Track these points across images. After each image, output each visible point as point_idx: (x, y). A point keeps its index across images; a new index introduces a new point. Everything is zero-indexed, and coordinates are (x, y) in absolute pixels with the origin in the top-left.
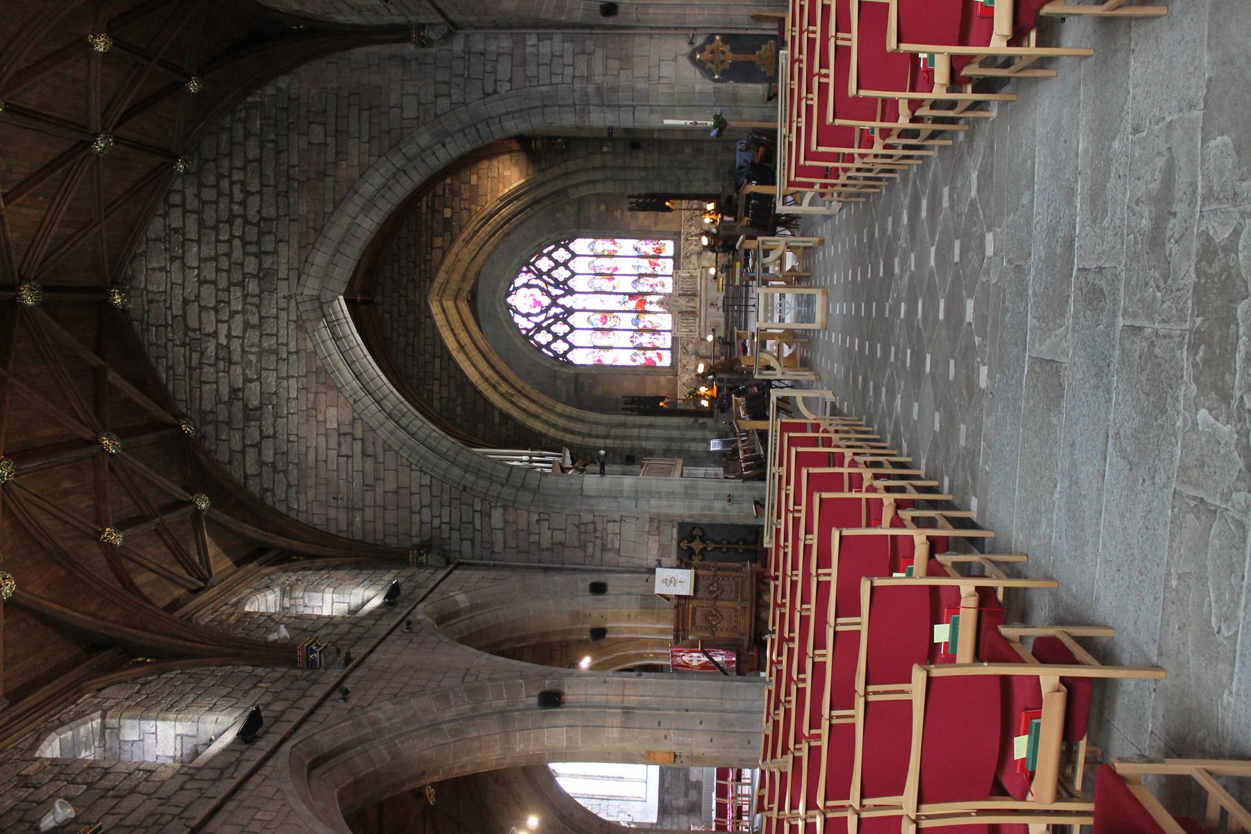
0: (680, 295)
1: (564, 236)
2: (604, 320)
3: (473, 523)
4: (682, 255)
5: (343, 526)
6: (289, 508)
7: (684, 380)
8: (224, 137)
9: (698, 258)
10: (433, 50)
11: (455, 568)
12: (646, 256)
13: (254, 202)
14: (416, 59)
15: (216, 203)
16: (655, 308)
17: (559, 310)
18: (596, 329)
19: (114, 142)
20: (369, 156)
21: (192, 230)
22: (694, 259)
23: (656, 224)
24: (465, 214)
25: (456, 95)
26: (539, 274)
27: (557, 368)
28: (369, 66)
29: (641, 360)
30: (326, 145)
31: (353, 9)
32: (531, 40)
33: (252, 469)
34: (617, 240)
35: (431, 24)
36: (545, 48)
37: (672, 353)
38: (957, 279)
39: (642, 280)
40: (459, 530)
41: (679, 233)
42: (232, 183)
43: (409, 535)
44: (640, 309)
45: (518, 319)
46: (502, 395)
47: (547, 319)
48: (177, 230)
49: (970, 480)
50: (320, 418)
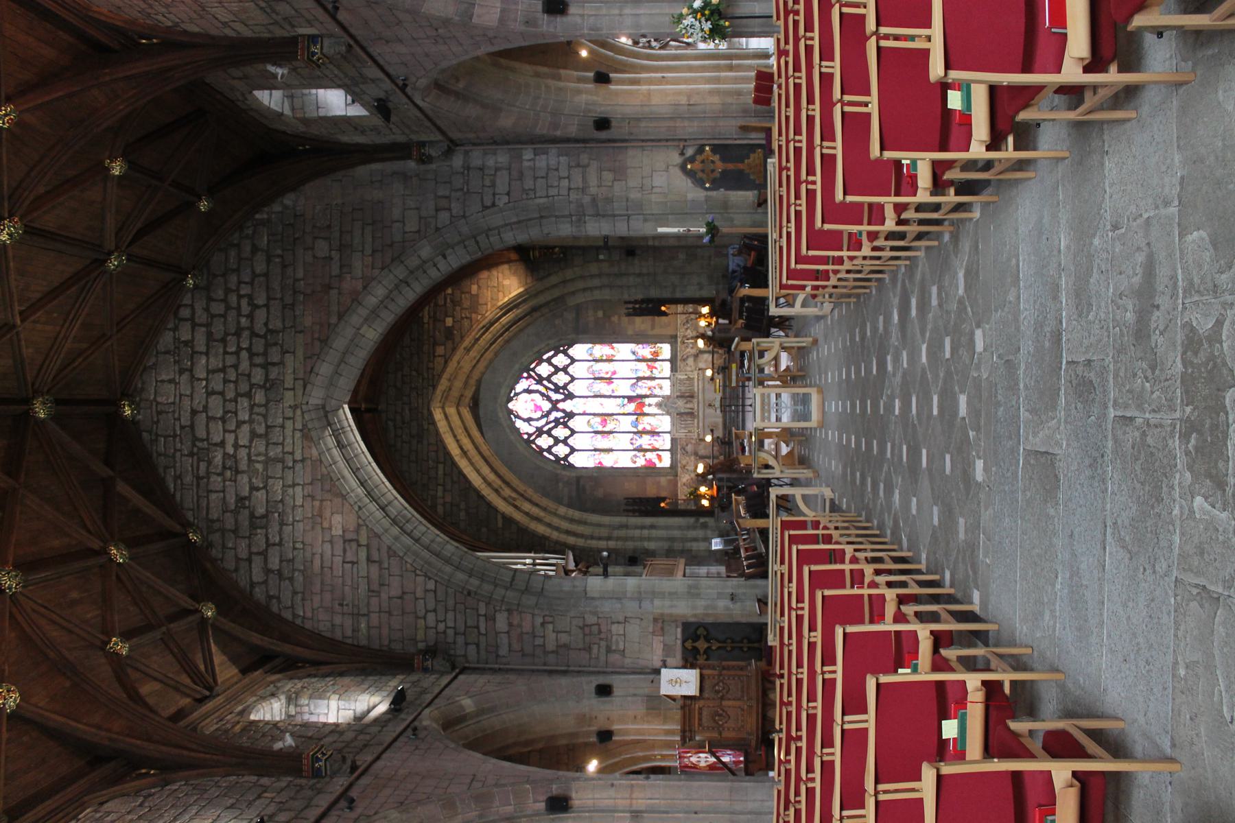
0: (677, 397)
1: (562, 342)
2: (604, 423)
3: (477, 627)
4: (679, 358)
5: (349, 633)
6: (295, 615)
7: (684, 480)
8: (233, 253)
9: (695, 360)
10: (433, 166)
11: (461, 673)
12: (643, 360)
13: (261, 315)
14: (417, 175)
15: (224, 316)
16: (654, 410)
17: (560, 415)
18: (596, 432)
19: (128, 259)
20: (373, 268)
21: (200, 343)
22: (690, 361)
23: (653, 328)
24: (466, 323)
25: (456, 208)
26: (540, 380)
27: (559, 472)
28: (372, 182)
29: (641, 462)
30: (331, 258)
31: (356, 129)
32: (528, 155)
33: (258, 576)
34: (614, 345)
35: (431, 143)
36: (542, 162)
37: (672, 455)
38: (949, 374)
39: (640, 383)
40: (464, 634)
41: (675, 337)
42: (240, 297)
43: (414, 641)
45: (519, 424)
46: (505, 499)
47: (547, 423)
48: (186, 343)
49: (971, 573)
50: (326, 525)
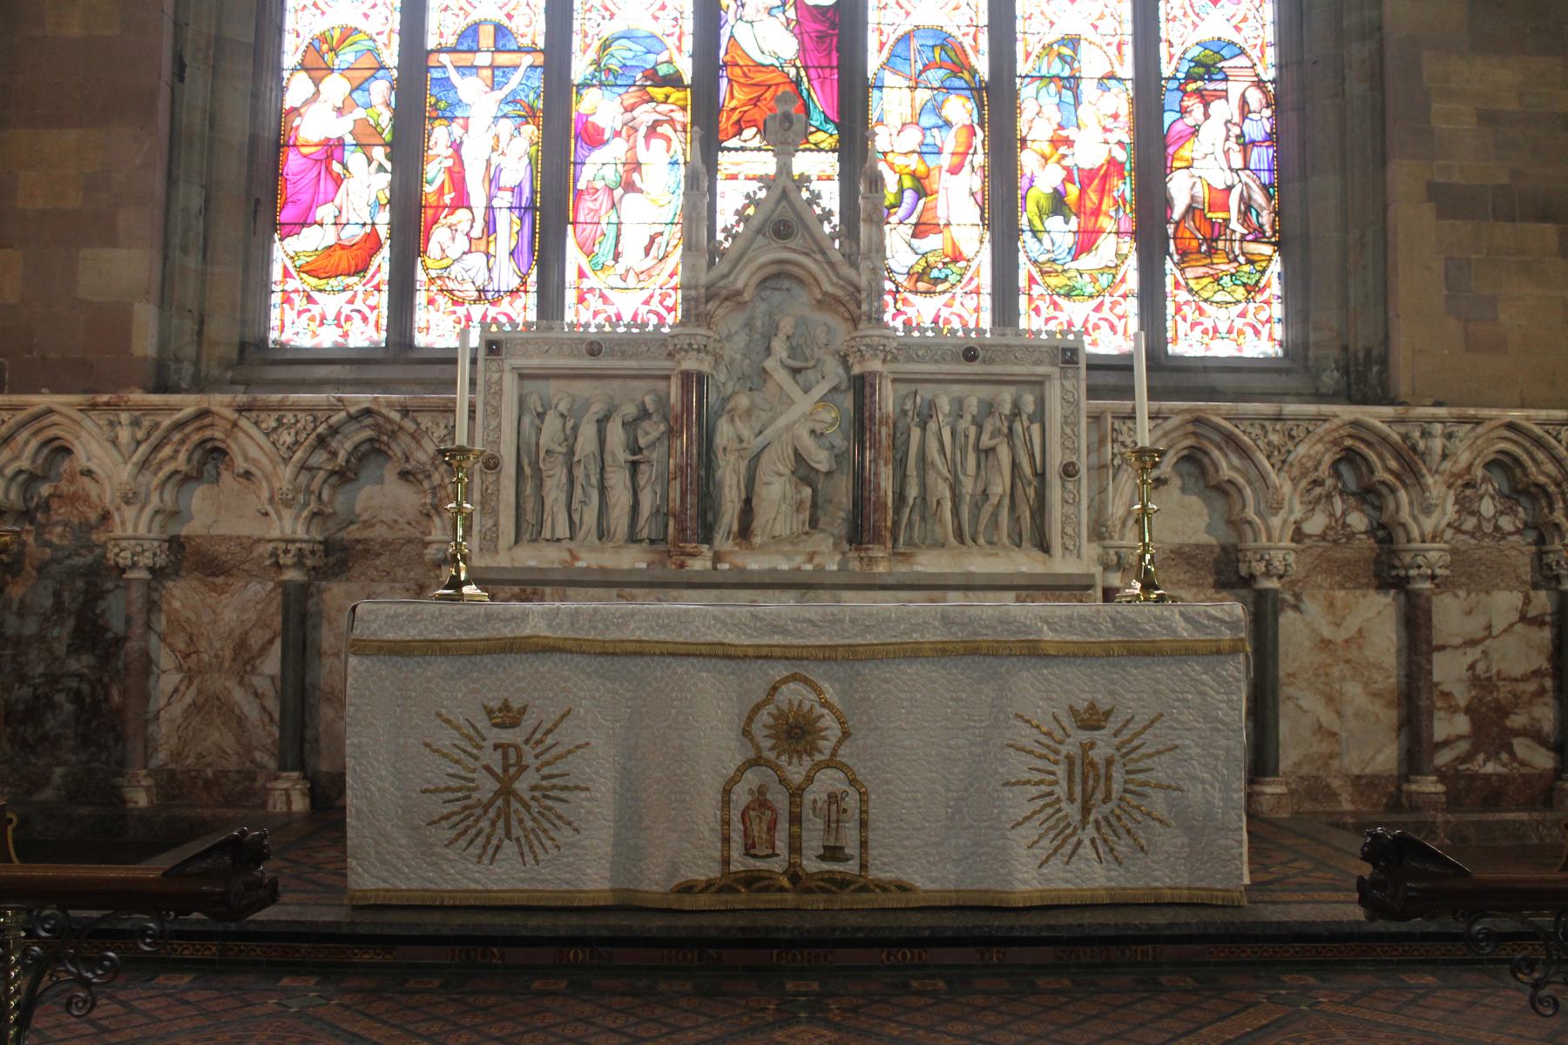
0: (861, 386)
4: (1218, 411)
9: (1184, 556)
39: (960, 109)
44: (731, 96)
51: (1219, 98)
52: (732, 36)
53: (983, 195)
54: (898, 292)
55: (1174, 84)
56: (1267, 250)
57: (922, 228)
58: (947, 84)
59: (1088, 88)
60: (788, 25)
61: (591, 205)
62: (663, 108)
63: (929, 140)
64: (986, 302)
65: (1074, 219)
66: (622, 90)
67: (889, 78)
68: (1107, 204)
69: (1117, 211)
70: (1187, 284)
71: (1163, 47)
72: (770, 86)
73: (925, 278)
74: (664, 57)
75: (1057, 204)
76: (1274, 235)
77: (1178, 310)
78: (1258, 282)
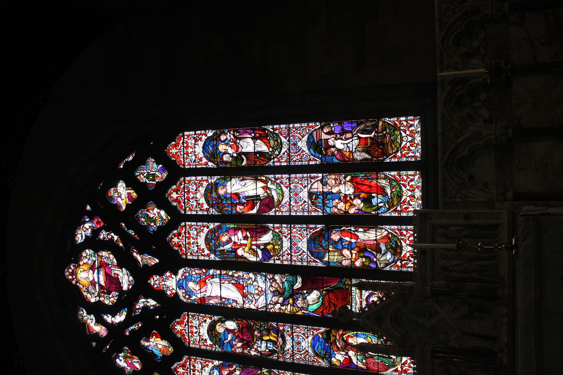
51: (328, 142)
52: (313, 312)
53: (365, 227)
54: (401, 259)
55: (324, 159)
56: (381, 123)
57: (378, 250)
58: (327, 239)
59: (325, 190)
60: (309, 293)
61: (372, 365)
62: (338, 337)
63: (346, 246)
64: (404, 227)
65: (373, 195)
66: (332, 351)
67: (326, 259)
68: (366, 182)
69: (369, 179)
70: (394, 153)
71: (311, 163)
72: (330, 300)
73: (396, 250)
74: (320, 336)
75: (367, 201)
76: (375, 121)
77: (404, 156)
78: (392, 126)
